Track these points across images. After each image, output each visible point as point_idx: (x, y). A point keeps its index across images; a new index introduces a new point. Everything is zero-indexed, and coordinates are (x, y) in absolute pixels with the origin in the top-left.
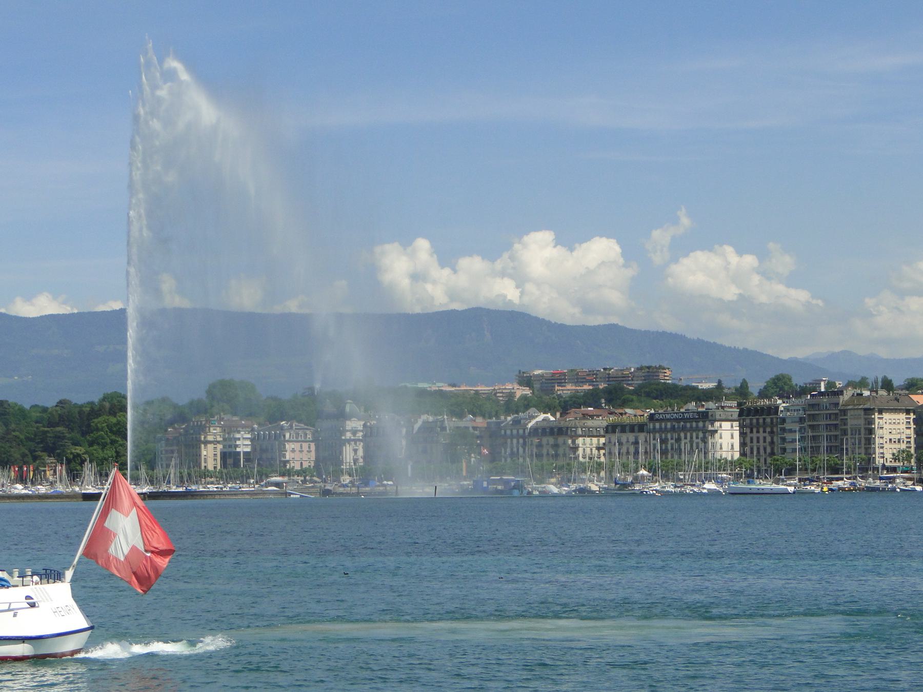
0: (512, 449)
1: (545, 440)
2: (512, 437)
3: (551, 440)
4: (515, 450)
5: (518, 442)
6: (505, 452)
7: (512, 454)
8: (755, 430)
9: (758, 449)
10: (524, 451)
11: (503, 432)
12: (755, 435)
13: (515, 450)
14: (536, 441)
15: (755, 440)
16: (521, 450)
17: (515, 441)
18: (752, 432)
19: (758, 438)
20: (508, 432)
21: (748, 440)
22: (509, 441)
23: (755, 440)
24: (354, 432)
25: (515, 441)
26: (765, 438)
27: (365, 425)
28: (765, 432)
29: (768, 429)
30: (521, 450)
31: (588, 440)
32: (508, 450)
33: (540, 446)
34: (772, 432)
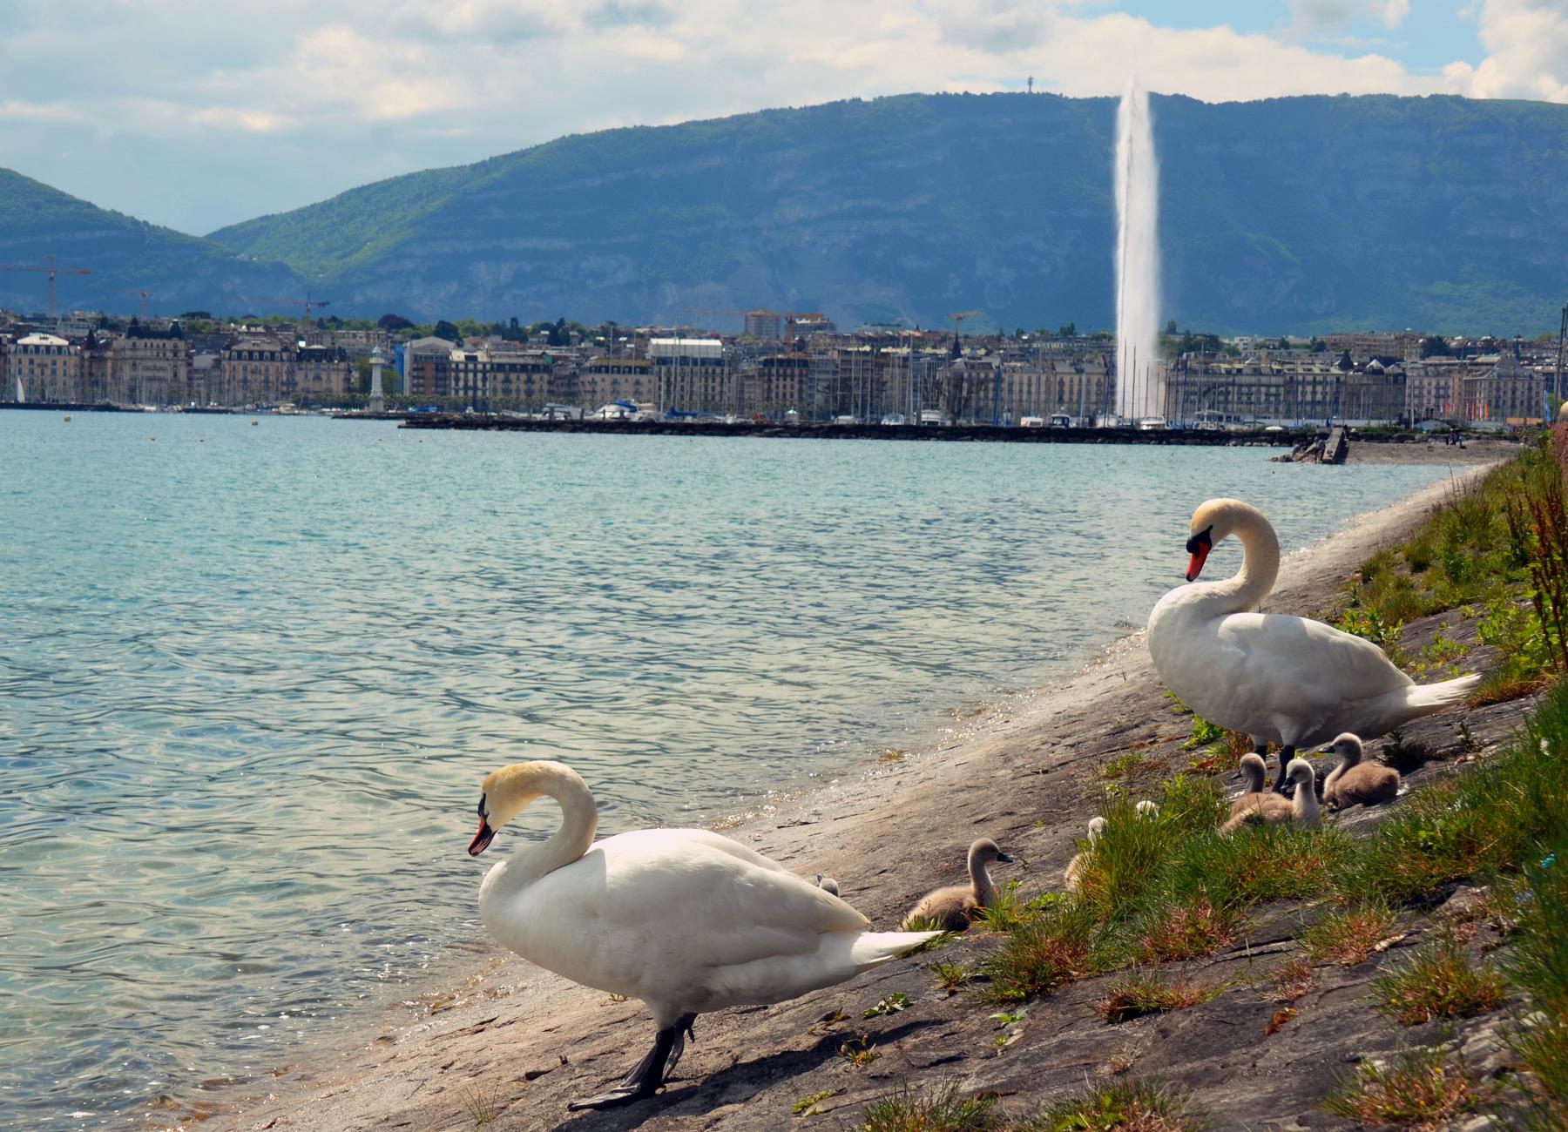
0: (466, 381)
2: (466, 371)
4: (471, 383)
5: (475, 376)
6: (457, 384)
10: (484, 385)
11: (453, 366)
12: (781, 383)
13: (471, 383)
16: (480, 384)
17: (471, 376)
19: (785, 387)
21: (773, 386)
26: (792, 387)
29: (797, 379)
30: (480, 384)
32: (461, 384)
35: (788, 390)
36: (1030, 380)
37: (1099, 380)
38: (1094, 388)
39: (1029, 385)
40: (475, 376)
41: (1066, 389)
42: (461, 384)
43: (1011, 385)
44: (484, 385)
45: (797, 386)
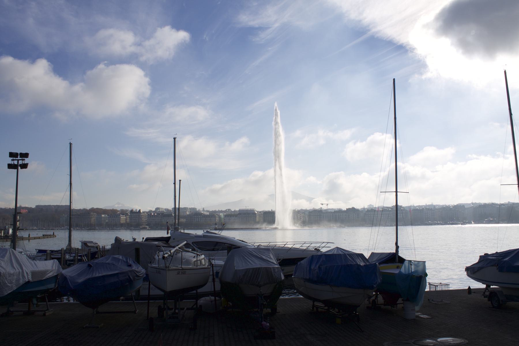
0: (197, 220)
4: (198, 220)
5: (199, 219)
10: (201, 221)
13: (198, 220)
17: (198, 219)
22: (196, 219)
25: (198, 219)
30: (200, 221)
32: (196, 221)
40: (199, 219)
42: (196, 221)
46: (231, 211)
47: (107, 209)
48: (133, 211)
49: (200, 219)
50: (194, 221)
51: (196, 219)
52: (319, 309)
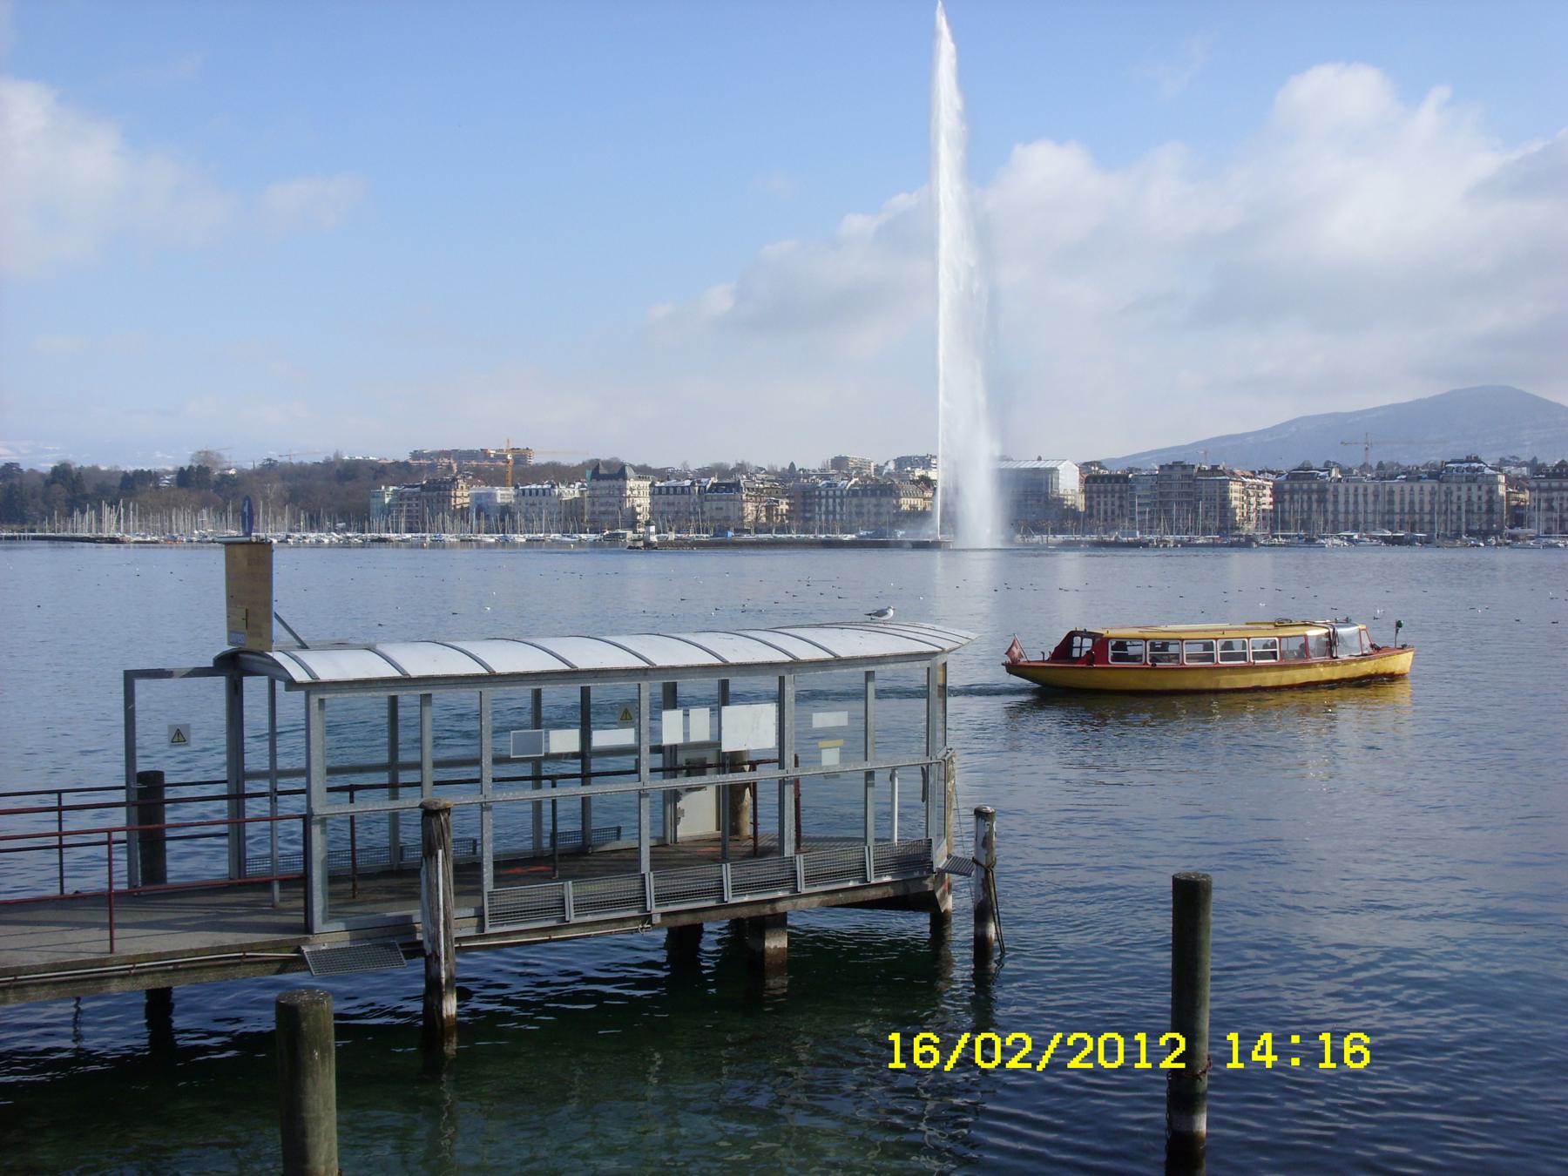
0: (827, 507)
1: (865, 501)
2: (827, 497)
3: (873, 501)
4: (831, 508)
5: (834, 501)
6: (820, 508)
7: (827, 512)
8: (1102, 496)
9: (1106, 512)
10: (842, 509)
11: (817, 493)
12: (1102, 500)
13: (831, 508)
14: (855, 501)
15: (1102, 504)
16: (838, 509)
17: (831, 501)
18: (1099, 497)
19: (1106, 504)
20: (823, 493)
21: (1095, 503)
22: (824, 501)
23: (1102, 504)
24: (632, 490)
25: (831, 501)
27: (652, 485)
28: (1113, 497)
29: (1117, 495)
30: (838, 509)
31: (905, 499)
32: (823, 508)
33: (860, 506)
34: (1121, 498)
35: (1109, 507)
36: (1356, 489)
37: (1433, 488)
38: (1427, 498)
39: (1356, 496)
40: (834, 501)
41: (1397, 498)
42: (823, 508)
43: (1336, 496)
44: (842, 509)
45: (1117, 503)
46: (42, 475)
47: (308, 460)
48: (602, 471)
49: (838, 500)
50: (817, 509)
51: (824, 501)
52: (114, 834)
